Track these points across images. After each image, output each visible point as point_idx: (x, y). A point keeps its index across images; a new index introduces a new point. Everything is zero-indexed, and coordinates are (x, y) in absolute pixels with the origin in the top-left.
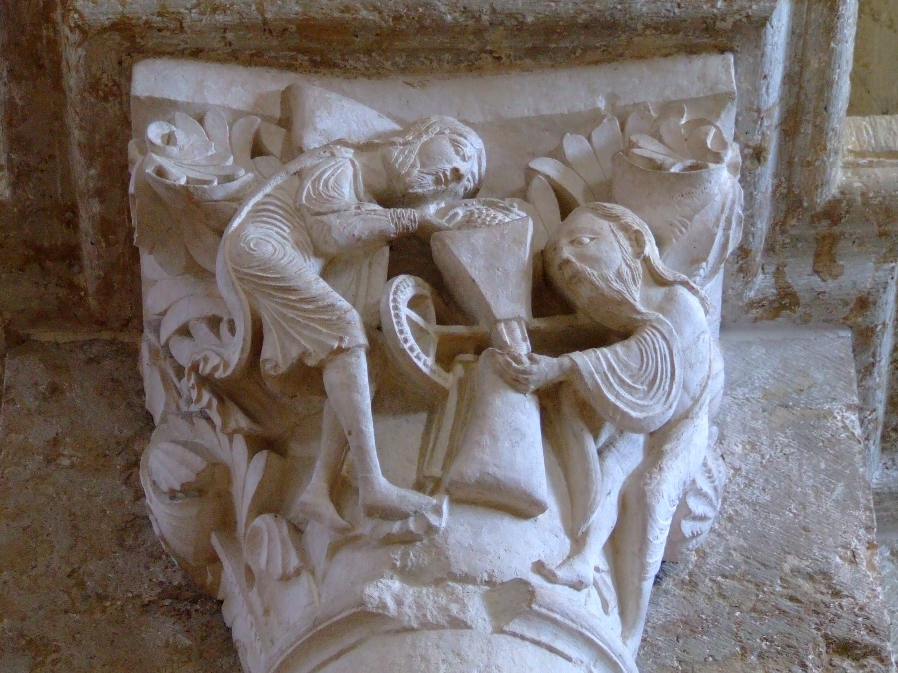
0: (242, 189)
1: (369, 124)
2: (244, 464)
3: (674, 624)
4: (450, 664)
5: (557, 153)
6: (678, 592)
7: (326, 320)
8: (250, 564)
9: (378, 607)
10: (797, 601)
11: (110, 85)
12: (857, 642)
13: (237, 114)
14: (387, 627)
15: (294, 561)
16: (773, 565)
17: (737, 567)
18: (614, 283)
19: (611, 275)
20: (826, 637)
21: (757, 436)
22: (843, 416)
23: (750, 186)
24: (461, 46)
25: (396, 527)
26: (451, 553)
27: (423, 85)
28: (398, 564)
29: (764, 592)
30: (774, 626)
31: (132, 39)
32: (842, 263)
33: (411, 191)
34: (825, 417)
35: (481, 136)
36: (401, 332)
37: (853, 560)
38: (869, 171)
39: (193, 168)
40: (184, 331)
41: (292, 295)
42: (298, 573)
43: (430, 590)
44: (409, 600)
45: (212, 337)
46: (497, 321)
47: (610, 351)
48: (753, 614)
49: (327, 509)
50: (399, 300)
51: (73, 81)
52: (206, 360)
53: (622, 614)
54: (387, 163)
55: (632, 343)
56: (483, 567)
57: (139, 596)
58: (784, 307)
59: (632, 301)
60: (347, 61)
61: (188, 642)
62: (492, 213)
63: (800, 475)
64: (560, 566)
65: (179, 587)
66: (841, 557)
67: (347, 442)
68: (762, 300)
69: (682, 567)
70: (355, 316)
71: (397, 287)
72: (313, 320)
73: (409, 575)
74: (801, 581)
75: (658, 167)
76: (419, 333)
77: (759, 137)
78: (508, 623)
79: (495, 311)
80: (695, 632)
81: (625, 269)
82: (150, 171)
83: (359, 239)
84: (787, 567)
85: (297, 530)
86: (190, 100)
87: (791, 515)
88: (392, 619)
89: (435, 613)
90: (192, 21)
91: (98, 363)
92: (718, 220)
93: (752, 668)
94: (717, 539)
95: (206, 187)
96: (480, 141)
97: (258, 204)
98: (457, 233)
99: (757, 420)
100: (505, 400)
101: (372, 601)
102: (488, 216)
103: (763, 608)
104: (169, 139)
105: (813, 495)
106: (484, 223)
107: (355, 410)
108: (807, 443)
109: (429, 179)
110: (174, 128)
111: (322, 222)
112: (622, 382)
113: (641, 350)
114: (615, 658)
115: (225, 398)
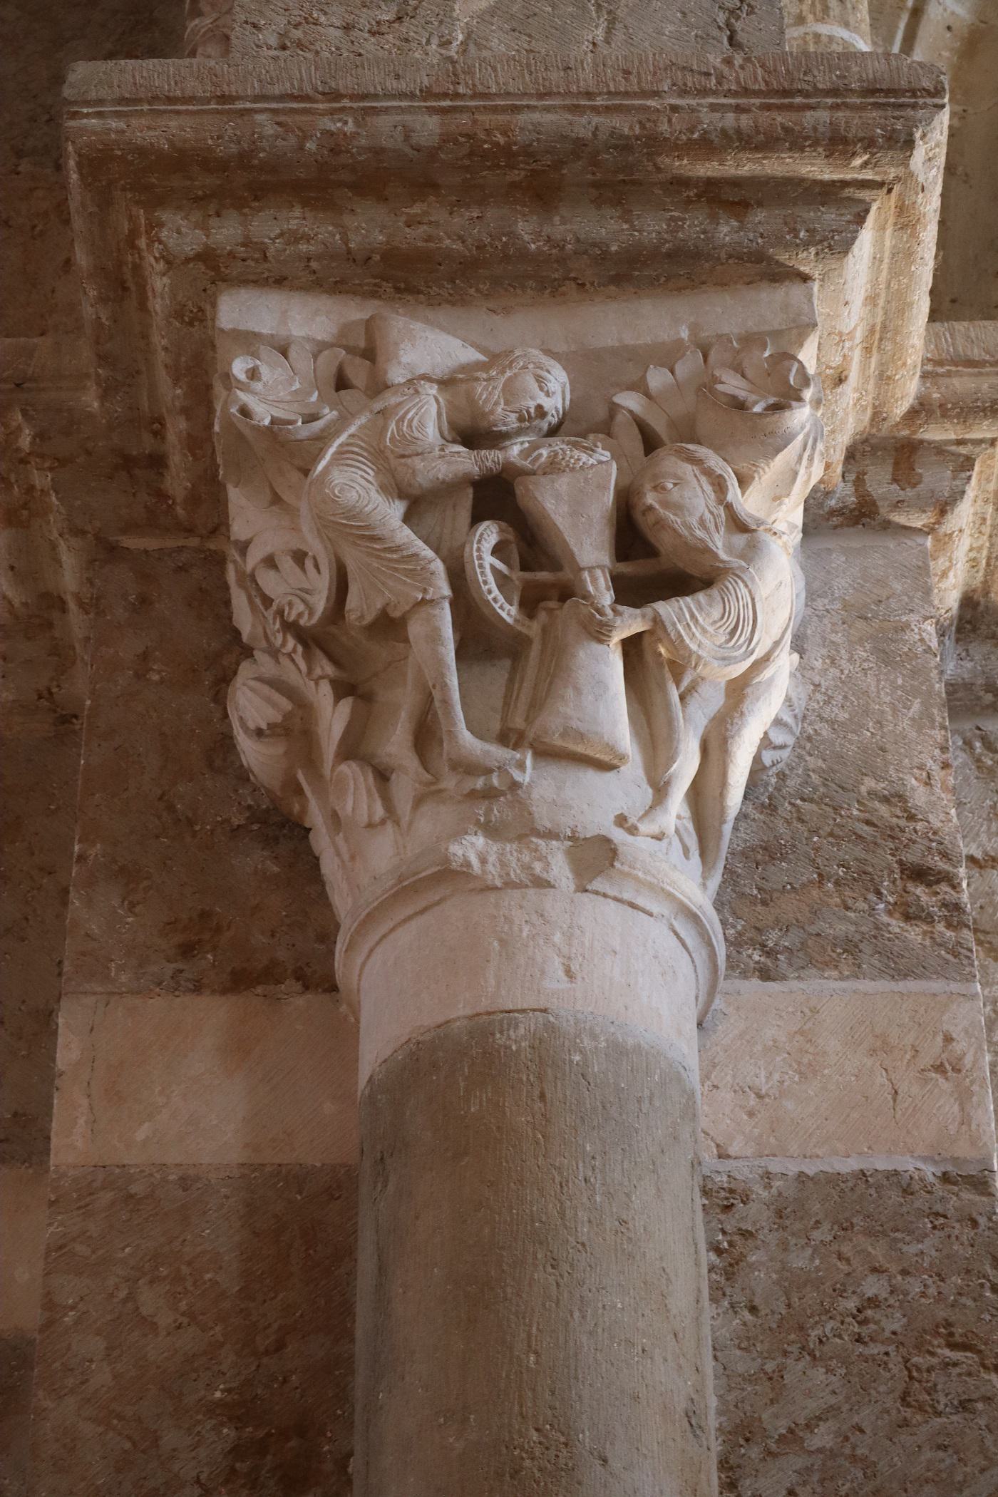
0: (327, 427)
1: (453, 355)
2: (330, 708)
3: (753, 850)
4: (533, 925)
5: (639, 386)
6: (757, 816)
7: (411, 570)
8: (337, 808)
9: (462, 865)
10: (875, 826)
11: (195, 310)
12: (931, 869)
13: (320, 348)
14: (471, 886)
15: (379, 811)
16: (851, 787)
17: (815, 789)
18: (697, 531)
19: (694, 522)
20: (900, 862)
21: (836, 650)
22: (920, 629)
23: (830, 404)
24: (545, 274)
25: (480, 783)
26: (534, 808)
27: (507, 311)
28: (482, 819)
29: (841, 815)
30: (851, 851)
31: (216, 268)
32: (920, 471)
33: (495, 429)
34: (903, 630)
35: (564, 369)
36: (485, 583)
37: (928, 782)
38: (947, 381)
39: (277, 404)
40: (270, 562)
41: (375, 543)
42: (383, 822)
43: (514, 846)
44: (492, 858)
45: (297, 570)
46: (581, 569)
47: (693, 599)
48: (830, 839)
49: (410, 762)
50: (483, 549)
51: (158, 305)
52: (290, 604)
53: (703, 854)
54: (471, 400)
55: (714, 592)
56: (566, 823)
57: (228, 821)
58: (864, 515)
59: (715, 550)
60: (431, 288)
61: (276, 869)
62: (576, 453)
63: (878, 692)
64: (641, 819)
65: (268, 810)
66: (916, 779)
67: (431, 694)
68: (842, 508)
69: (762, 790)
70: (438, 566)
71: (482, 535)
72: (396, 570)
73: (492, 830)
74: (877, 804)
75: (739, 405)
76: (502, 580)
77: (841, 359)
78: (591, 882)
79: (578, 558)
80: (774, 859)
81: (708, 516)
82: (234, 410)
83: (443, 482)
84: (863, 789)
85: (383, 776)
86: (274, 332)
87: (869, 734)
88: (476, 877)
89: (518, 871)
90: (277, 251)
91: (187, 571)
93: (828, 896)
94: (796, 760)
95: (290, 427)
96: (564, 374)
97: (341, 445)
98: (543, 480)
99: (837, 633)
100: (589, 652)
101: (456, 859)
102: (571, 457)
103: (841, 833)
104: (253, 374)
105: (890, 713)
106: (568, 466)
107: (439, 662)
108: (886, 657)
109: (513, 417)
110: (258, 362)
111: (406, 465)
112: (704, 631)
113: (723, 599)
114: (695, 910)
115: (310, 642)
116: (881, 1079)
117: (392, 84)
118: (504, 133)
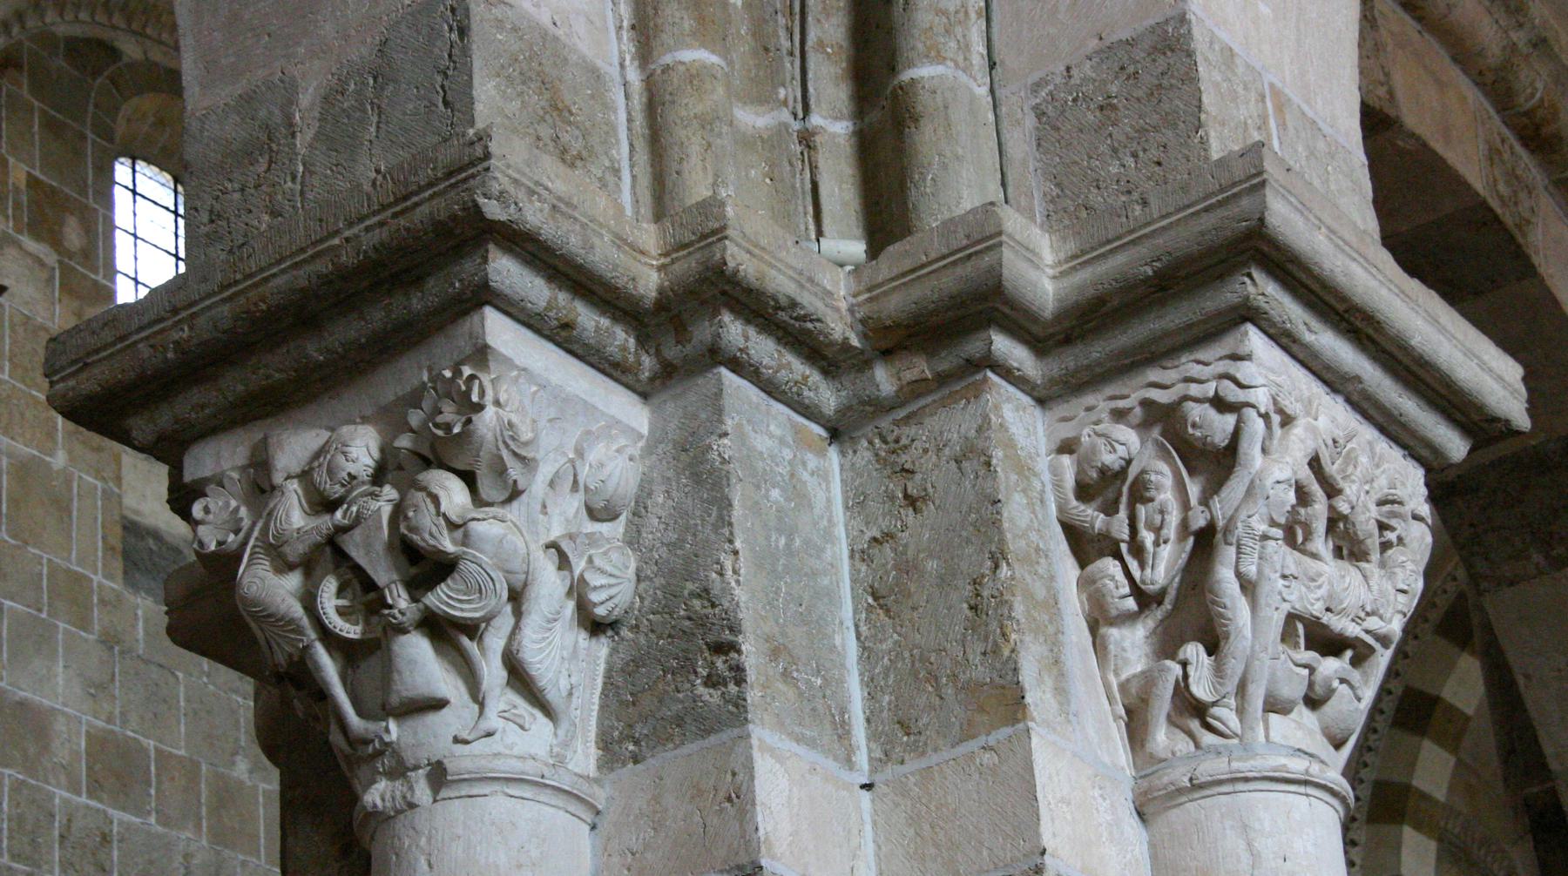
13: (243, 469)
19: (427, 536)
20: (707, 644)
44: (388, 797)
55: (456, 575)
75: (448, 427)
84: (686, 593)
92: (497, 447)
104: (207, 510)
112: (461, 601)
116: (697, 818)
117: (204, 288)
118: (263, 301)
